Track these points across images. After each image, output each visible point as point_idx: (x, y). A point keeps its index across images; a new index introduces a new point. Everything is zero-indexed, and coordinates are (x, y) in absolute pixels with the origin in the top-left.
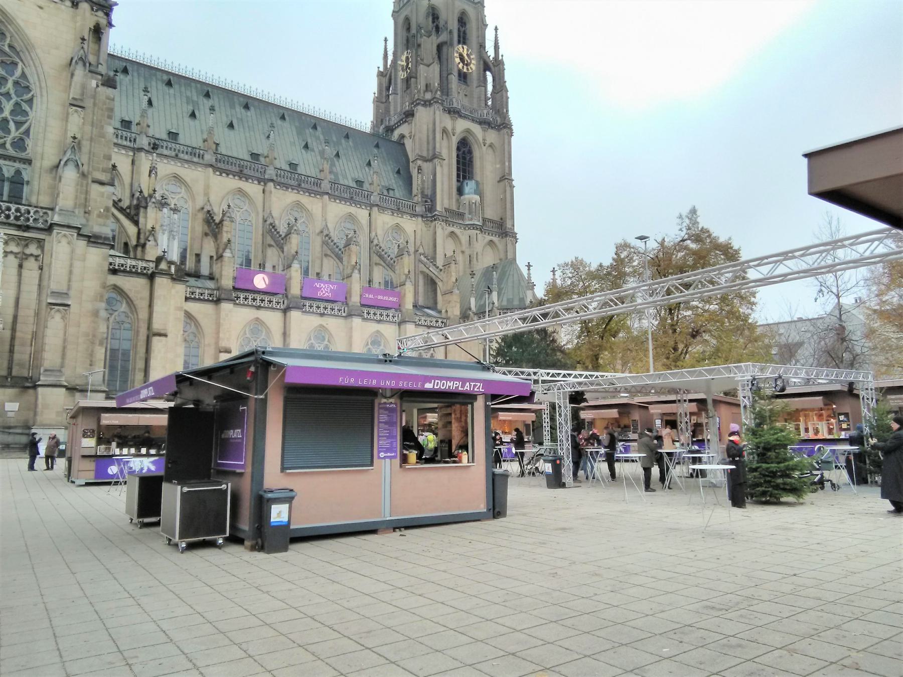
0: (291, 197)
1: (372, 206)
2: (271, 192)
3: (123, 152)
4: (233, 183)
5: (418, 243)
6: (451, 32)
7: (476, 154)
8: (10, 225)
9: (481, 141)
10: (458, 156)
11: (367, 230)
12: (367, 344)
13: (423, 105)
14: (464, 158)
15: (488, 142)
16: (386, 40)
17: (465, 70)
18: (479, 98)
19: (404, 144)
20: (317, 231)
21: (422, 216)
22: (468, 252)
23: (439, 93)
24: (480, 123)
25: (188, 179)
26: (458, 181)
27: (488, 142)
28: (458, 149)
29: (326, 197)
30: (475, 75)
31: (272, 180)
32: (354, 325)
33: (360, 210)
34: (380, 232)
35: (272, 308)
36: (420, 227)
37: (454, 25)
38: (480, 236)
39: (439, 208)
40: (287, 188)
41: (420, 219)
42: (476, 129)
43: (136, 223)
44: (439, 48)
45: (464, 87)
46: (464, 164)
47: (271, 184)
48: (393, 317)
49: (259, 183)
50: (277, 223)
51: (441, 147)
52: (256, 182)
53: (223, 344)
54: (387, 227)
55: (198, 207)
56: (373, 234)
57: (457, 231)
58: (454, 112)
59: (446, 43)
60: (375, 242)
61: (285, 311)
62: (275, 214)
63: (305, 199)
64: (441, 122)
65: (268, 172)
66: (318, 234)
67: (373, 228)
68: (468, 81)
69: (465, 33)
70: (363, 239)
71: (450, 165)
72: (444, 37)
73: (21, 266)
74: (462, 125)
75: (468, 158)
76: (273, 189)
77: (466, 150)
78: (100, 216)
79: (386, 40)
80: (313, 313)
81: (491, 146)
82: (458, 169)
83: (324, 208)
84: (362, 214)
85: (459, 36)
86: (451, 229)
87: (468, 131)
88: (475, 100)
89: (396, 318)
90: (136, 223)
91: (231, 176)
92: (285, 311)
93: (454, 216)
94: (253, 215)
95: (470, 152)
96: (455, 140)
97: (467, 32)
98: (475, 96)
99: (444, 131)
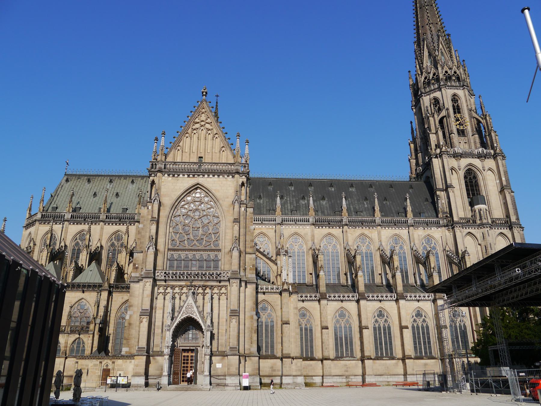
0: (359, 231)
1: (409, 227)
2: (347, 231)
3: (271, 227)
4: (325, 230)
5: (444, 244)
6: (447, 109)
7: (480, 177)
8: (214, 280)
9: (481, 169)
10: (466, 182)
11: (408, 242)
12: (413, 316)
13: (435, 158)
14: (472, 182)
15: (486, 168)
16: (411, 122)
17: (462, 128)
18: (475, 142)
19: (430, 182)
20: (376, 249)
21: (445, 226)
22: (483, 245)
23: (444, 148)
24: (478, 158)
25: (302, 234)
26: (468, 198)
27: (486, 168)
28: (465, 177)
29: (379, 227)
30: (469, 128)
31: (347, 225)
32: (401, 305)
33: (402, 231)
34: (417, 242)
35: (350, 300)
36: (444, 233)
37: (449, 104)
38: (489, 231)
39: (455, 219)
40: (356, 227)
41: (444, 228)
42: (476, 162)
43: (276, 264)
44: (441, 121)
45: (463, 138)
46: (472, 186)
47: (346, 227)
48: (429, 297)
49: (340, 228)
50: (351, 248)
51: (451, 180)
52: (338, 228)
53: (324, 324)
54: (421, 237)
55: (309, 248)
56: (412, 244)
57: (471, 230)
58: (457, 156)
59: (446, 116)
60: (414, 249)
61: (358, 301)
62: (350, 243)
63: (366, 231)
64: (448, 165)
65: (344, 220)
66: (377, 250)
67: (411, 240)
68: (466, 134)
69: (458, 106)
70: (407, 249)
71: (461, 189)
72: (443, 113)
73: (219, 299)
74: (464, 162)
75: (474, 182)
76: (348, 230)
77: (472, 177)
78: (250, 269)
79: (411, 122)
80: (374, 300)
81: (490, 169)
82: (467, 190)
83: (379, 233)
84: (403, 232)
85: (454, 109)
86: (468, 230)
87: (470, 165)
88: (473, 145)
89: (430, 298)
90: (276, 264)
91: (324, 227)
92: (358, 301)
93: (469, 223)
94: (338, 246)
95: (475, 177)
96: (462, 173)
97: (460, 105)
98: (472, 141)
99: (452, 169)
